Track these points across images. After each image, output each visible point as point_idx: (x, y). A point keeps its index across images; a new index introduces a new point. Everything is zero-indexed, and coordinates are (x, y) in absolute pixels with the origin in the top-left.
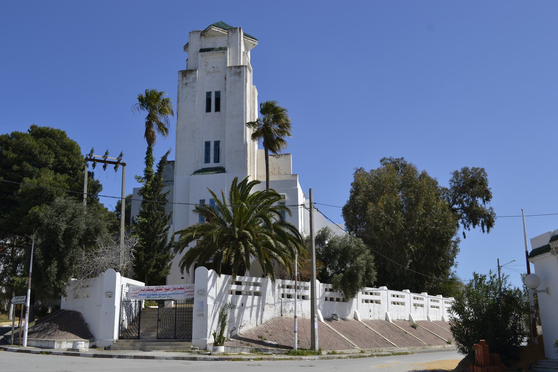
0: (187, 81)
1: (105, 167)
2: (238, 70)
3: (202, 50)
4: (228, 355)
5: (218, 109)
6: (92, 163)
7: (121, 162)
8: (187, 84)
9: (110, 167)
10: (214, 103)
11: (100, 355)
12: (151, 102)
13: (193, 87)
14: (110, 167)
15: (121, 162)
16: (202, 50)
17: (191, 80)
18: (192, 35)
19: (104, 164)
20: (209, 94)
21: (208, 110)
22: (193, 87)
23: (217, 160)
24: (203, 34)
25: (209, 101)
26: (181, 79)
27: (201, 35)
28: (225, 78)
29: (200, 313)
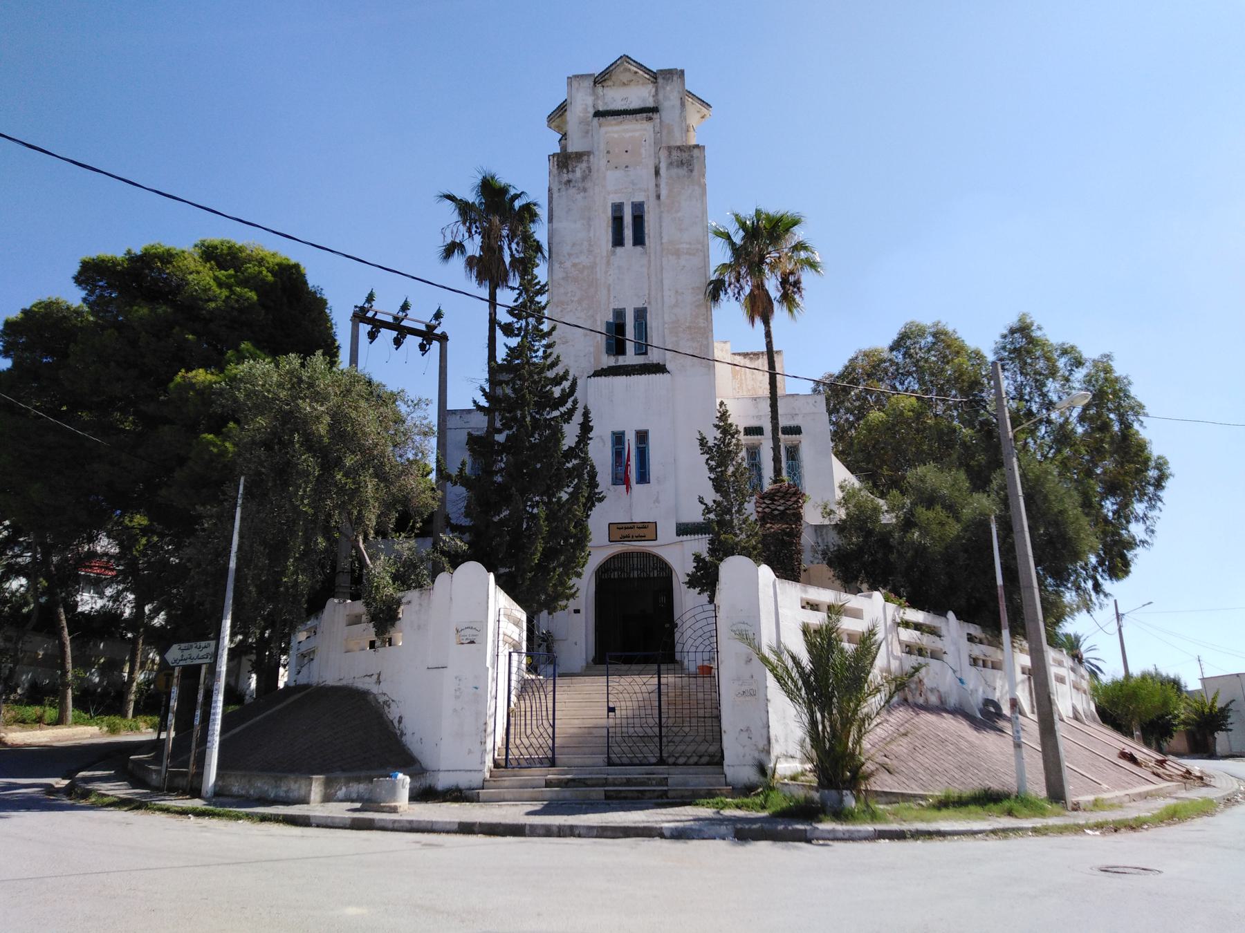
0: (571, 176)
1: (398, 342)
2: (685, 155)
3: (598, 114)
4: (1112, 806)
5: (639, 240)
6: (369, 328)
7: (438, 331)
8: (569, 181)
9: (412, 342)
10: (629, 227)
11: (503, 834)
12: (494, 208)
13: (585, 190)
14: (412, 342)
15: (438, 331)
16: (598, 114)
17: (578, 174)
18: (575, 84)
19: (395, 334)
20: (618, 209)
21: (618, 241)
22: (585, 190)
23: (642, 349)
24: (601, 80)
25: (618, 221)
26: (555, 171)
27: (595, 83)
28: (657, 173)
29: (744, 688)
